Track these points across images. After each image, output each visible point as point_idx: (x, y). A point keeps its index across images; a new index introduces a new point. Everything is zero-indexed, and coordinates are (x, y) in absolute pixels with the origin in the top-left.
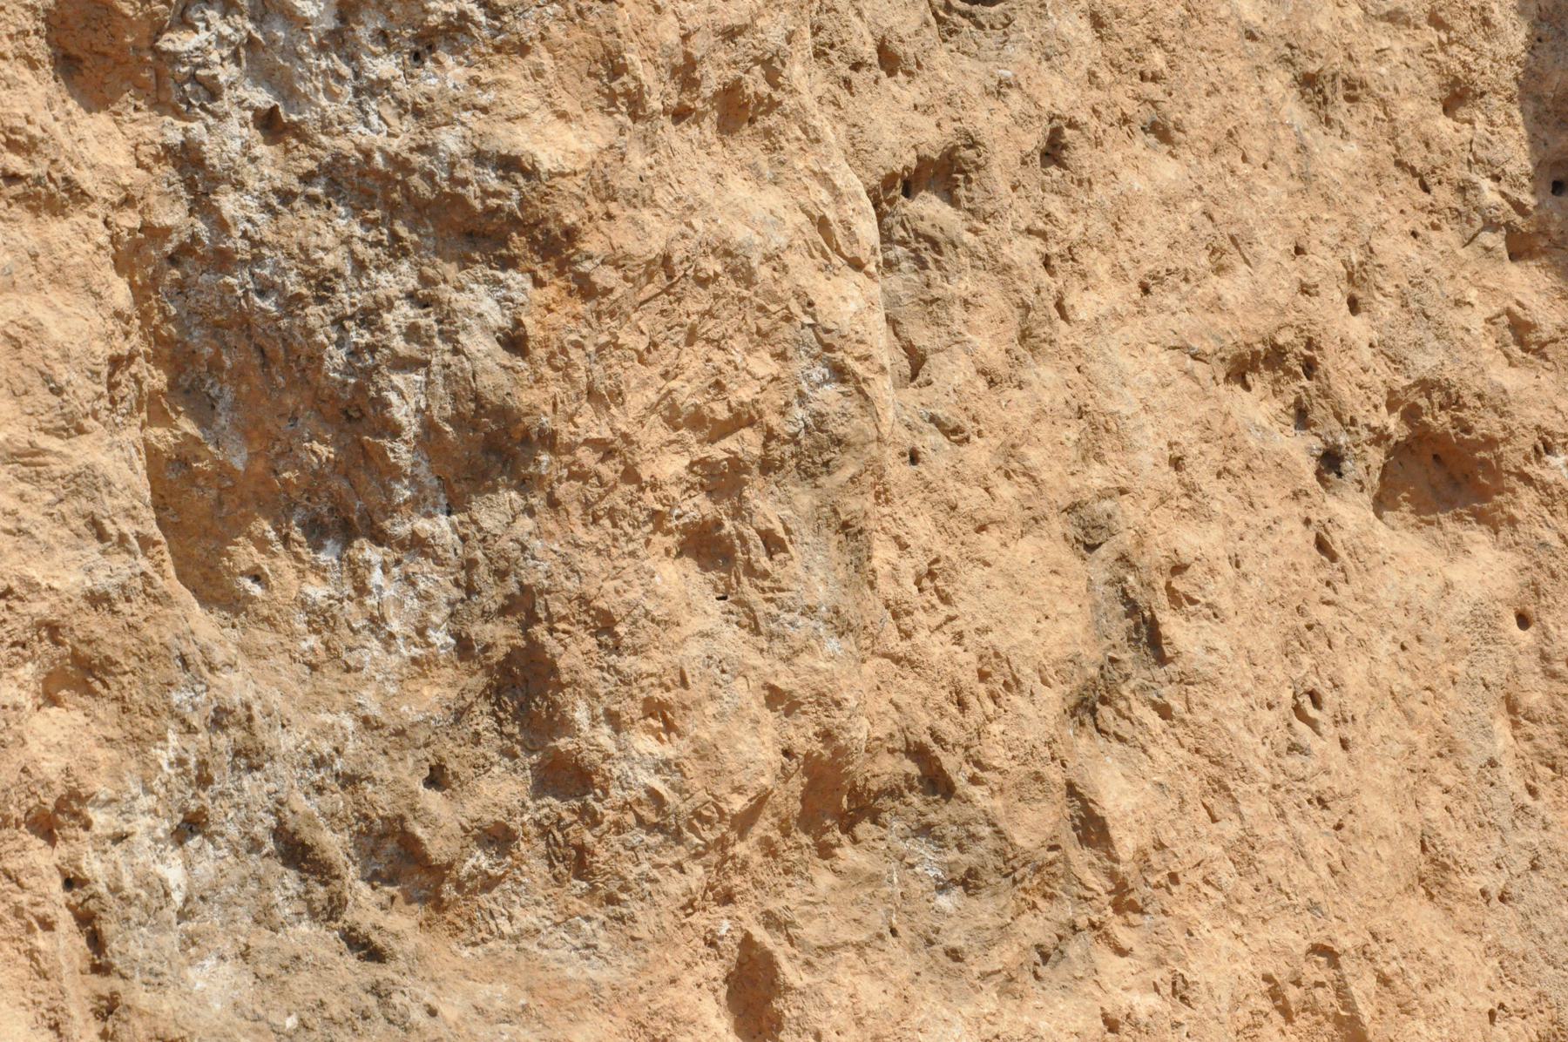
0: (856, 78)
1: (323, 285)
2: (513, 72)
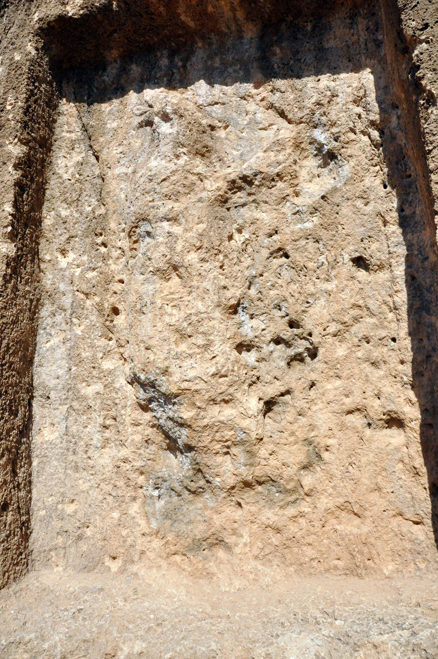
0: (266, 385)
1: (170, 429)
2: (182, 407)
